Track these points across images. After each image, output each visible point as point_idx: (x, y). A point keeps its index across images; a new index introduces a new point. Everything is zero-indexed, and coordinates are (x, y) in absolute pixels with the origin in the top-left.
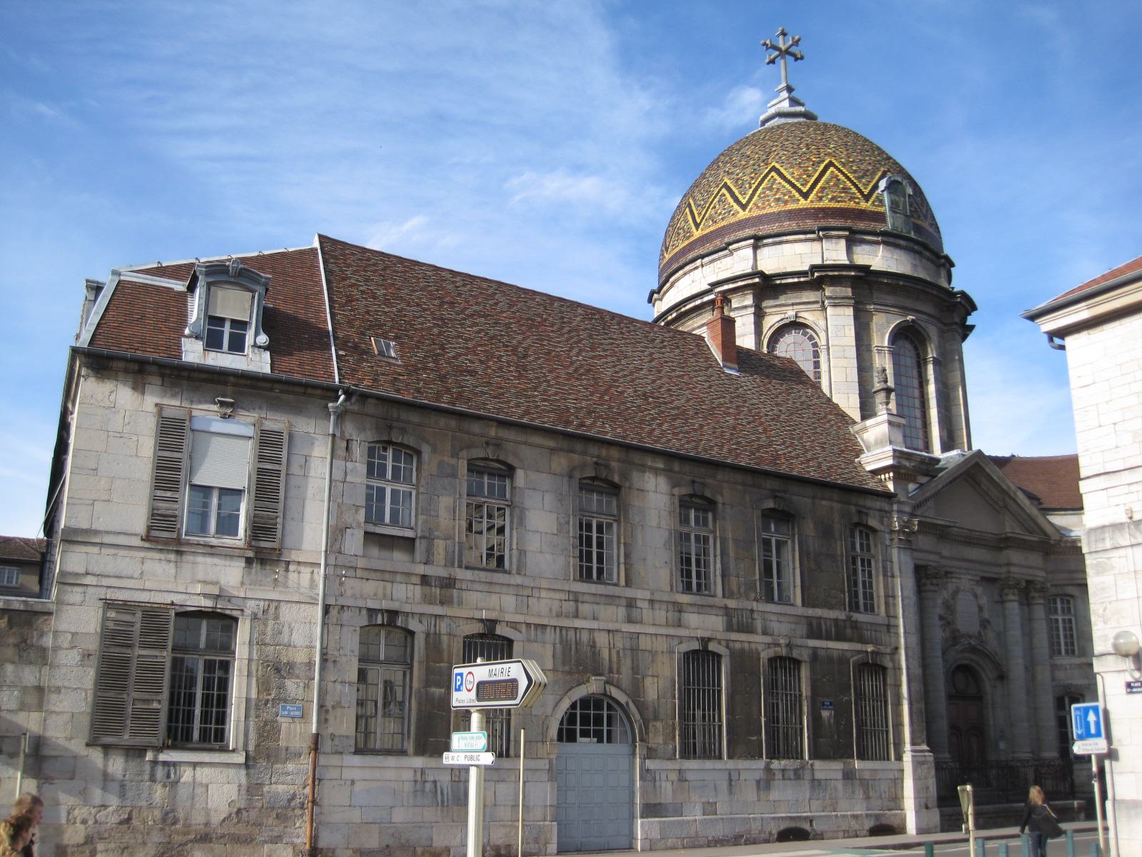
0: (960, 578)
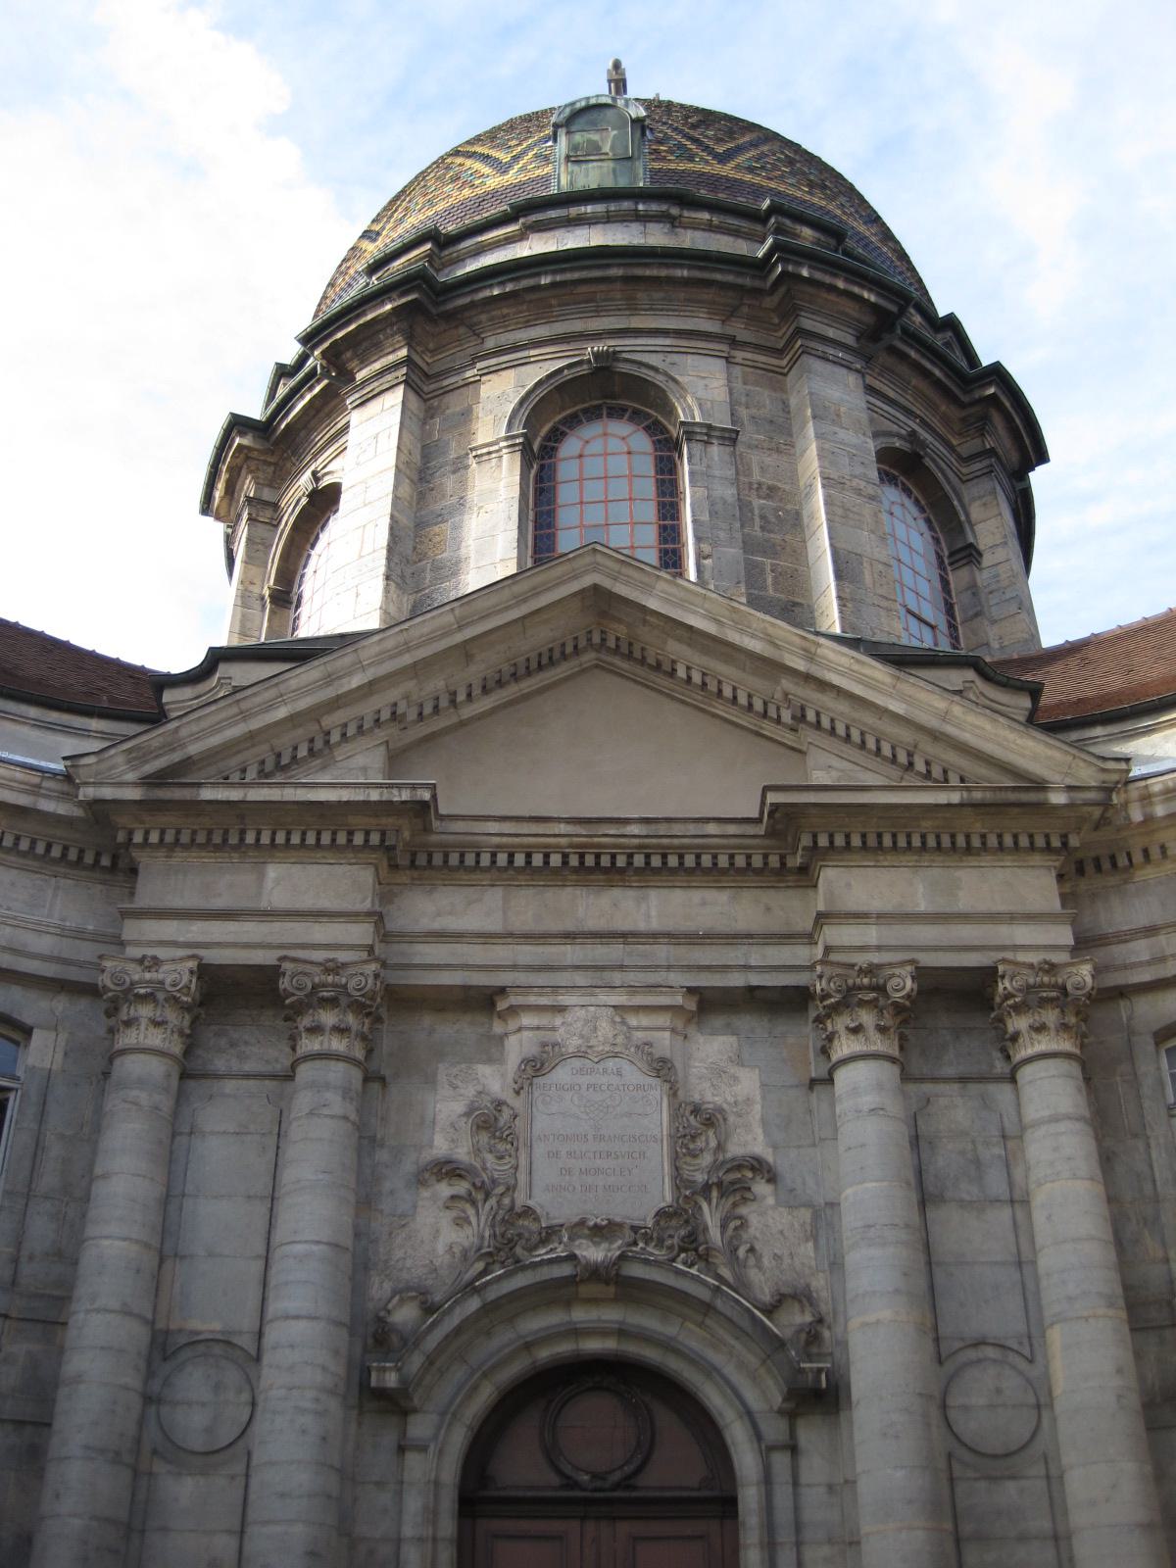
0: (561, 1009)
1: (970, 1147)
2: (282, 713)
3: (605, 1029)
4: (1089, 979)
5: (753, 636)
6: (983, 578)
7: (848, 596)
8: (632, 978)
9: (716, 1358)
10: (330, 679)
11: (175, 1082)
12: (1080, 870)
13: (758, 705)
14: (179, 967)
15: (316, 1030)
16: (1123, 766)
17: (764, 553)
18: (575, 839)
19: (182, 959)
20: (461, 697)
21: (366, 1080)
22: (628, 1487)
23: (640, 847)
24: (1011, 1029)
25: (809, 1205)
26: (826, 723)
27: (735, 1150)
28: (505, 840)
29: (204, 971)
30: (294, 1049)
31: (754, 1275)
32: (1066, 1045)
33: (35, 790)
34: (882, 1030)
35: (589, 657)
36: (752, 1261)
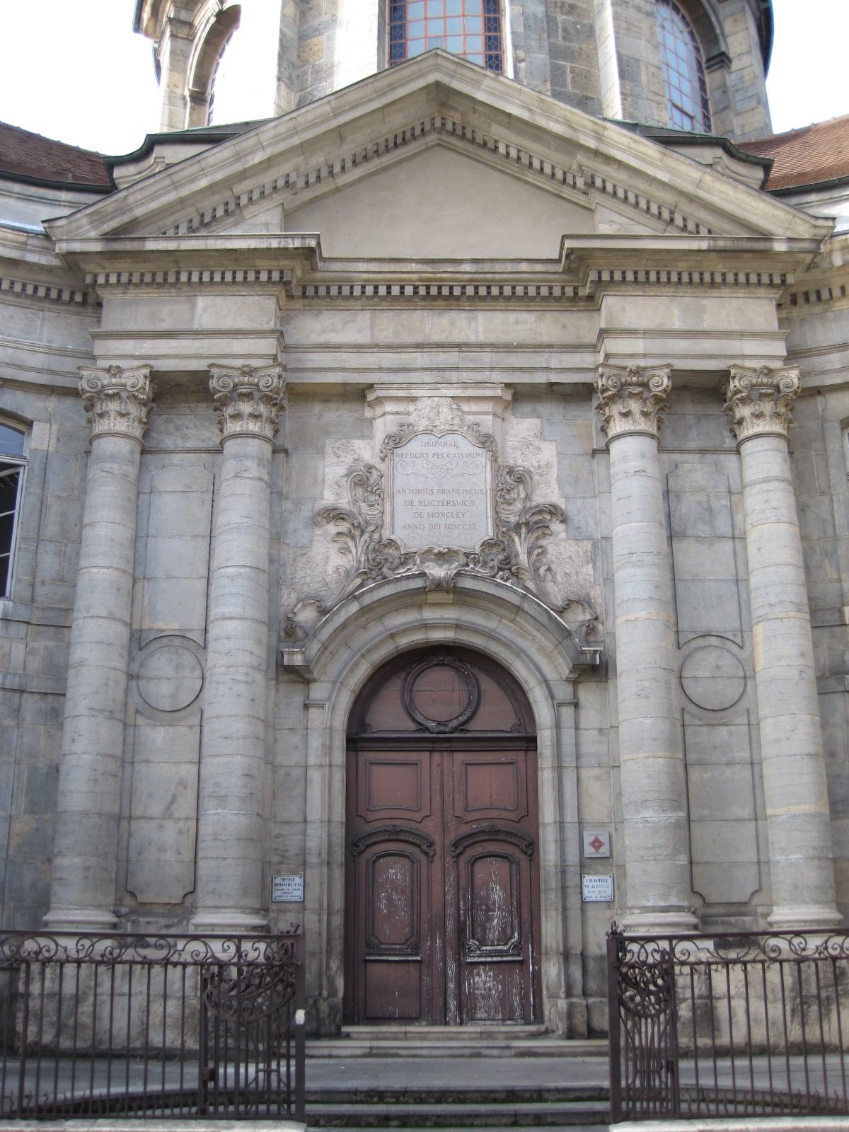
0: (413, 399)
1: (705, 499)
2: (203, 183)
3: (446, 414)
4: (796, 381)
5: (556, 121)
6: (731, 79)
7: (628, 92)
8: (465, 376)
9: (524, 644)
10: (238, 157)
11: (137, 456)
12: (794, 301)
13: (559, 175)
14: (136, 373)
15: (237, 416)
16: (830, 223)
17: (565, 59)
18: (424, 275)
19: (138, 368)
20: (337, 169)
21: (274, 452)
22: (462, 731)
23: (471, 280)
24: (738, 416)
25: (589, 539)
26: (609, 188)
27: (538, 500)
28: (371, 276)
29: (155, 376)
30: (222, 431)
31: (550, 587)
32: (777, 427)
33: (23, 246)
34: (645, 414)
35: (432, 138)
36: (549, 577)
